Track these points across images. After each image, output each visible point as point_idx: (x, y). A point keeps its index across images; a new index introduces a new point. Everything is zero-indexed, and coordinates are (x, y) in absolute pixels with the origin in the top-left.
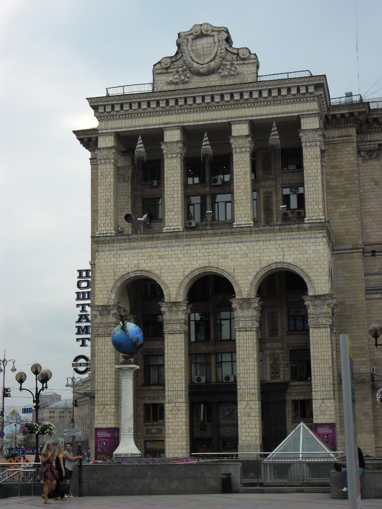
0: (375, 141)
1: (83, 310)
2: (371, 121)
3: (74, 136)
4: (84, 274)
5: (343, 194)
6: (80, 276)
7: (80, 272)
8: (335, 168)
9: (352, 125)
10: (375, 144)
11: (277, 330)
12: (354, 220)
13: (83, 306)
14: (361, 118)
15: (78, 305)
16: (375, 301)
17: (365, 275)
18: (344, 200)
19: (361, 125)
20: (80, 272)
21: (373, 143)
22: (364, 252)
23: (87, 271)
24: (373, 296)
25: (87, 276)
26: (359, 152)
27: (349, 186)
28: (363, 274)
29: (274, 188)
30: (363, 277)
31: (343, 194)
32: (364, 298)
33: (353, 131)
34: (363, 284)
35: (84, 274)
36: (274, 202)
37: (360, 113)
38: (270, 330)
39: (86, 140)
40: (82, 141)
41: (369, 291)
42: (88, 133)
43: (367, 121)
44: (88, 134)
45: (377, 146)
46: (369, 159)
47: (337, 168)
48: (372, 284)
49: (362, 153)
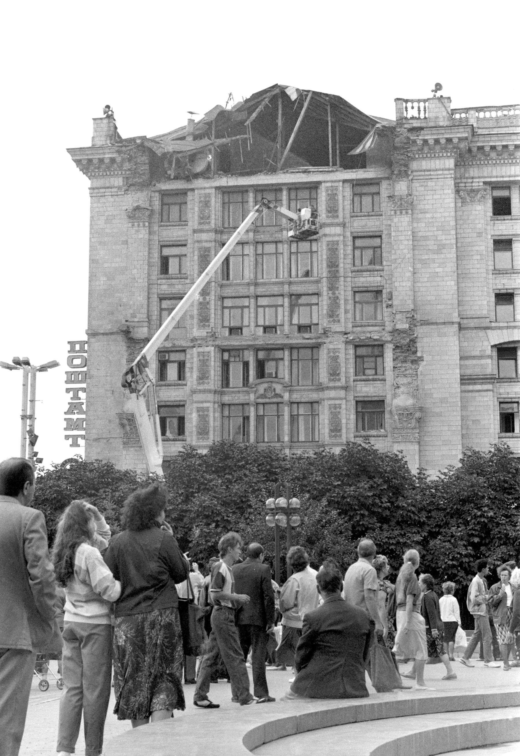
0: (479, 177)
1: (76, 397)
2: (475, 149)
3: (69, 157)
4: (77, 347)
5: (436, 247)
6: (72, 350)
7: (72, 344)
8: (425, 213)
9: (449, 154)
10: (479, 182)
11: (340, 430)
12: (448, 283)
13: (76, 391)
14: (462, 145)
15: (68, 390)
16: (474, 394)
17: (461, 358)
18: (436, 256)
19: (461, 155)
20: (72, 344)
21: (477, 180)
22: (460, 329)
23: (82, 343)
24: (471, 387)
25: (82, 350)
26: (457, 191)
27: (443, 237)
28: (459, 358)
29: (342, 238)
30: (458, 362)
31: (436, 247)
32: (459, 390)
33: (450, 163)
34: (458, 371)
35: (77, 347)
36: (342, 256)
37: (460, 139)
38: (331, 430)
39: (85, 162)
40: (78, 162)
41: (465, 380)
42: (88, 152)
43: (470, 150)
44: (87, 155)
45: (482, 184)
46: (471, 201)
47: (427, 213)
48: (469, 372)
49: (462, 193)
